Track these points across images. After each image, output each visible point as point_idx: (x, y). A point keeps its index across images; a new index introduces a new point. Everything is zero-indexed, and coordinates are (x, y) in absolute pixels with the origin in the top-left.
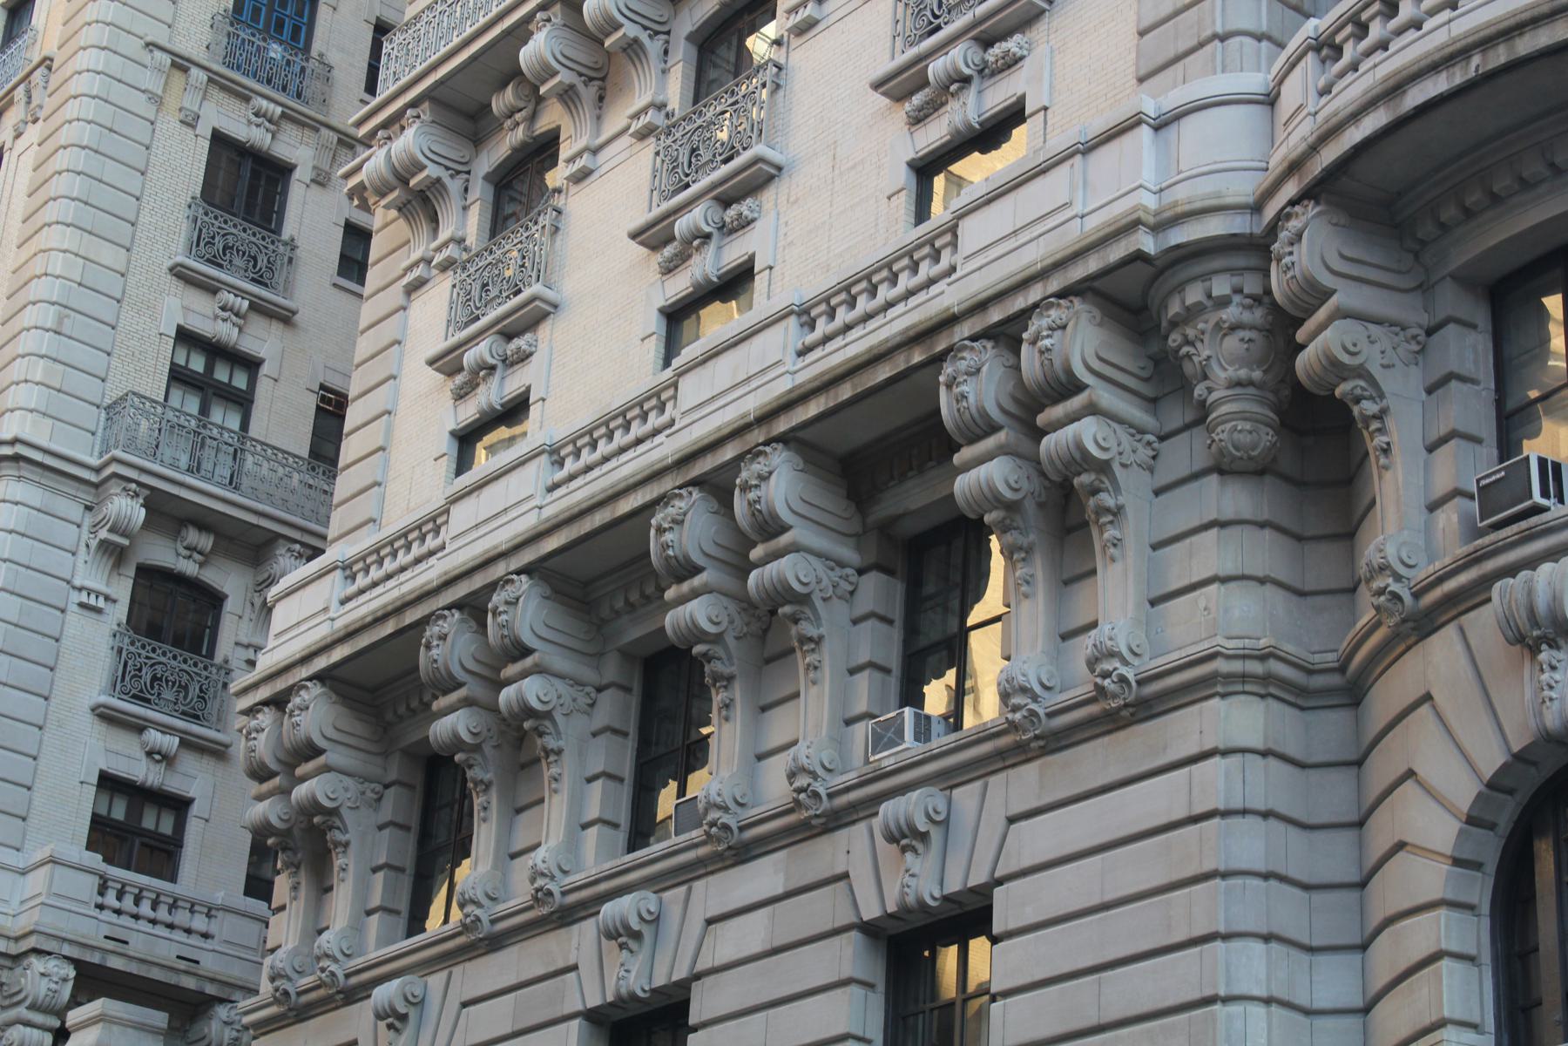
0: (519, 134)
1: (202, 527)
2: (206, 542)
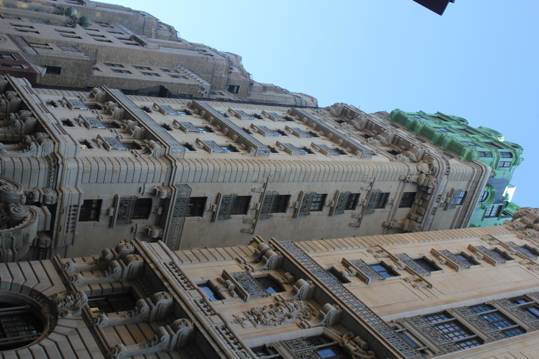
0: (282, 281)
1: (163, 211)
2: (160, 212)
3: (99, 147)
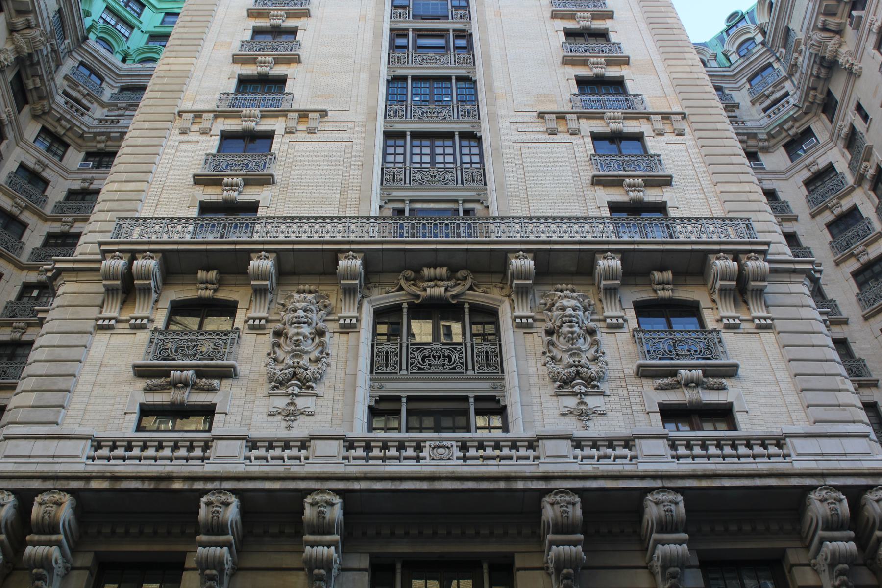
0: (208, 293)
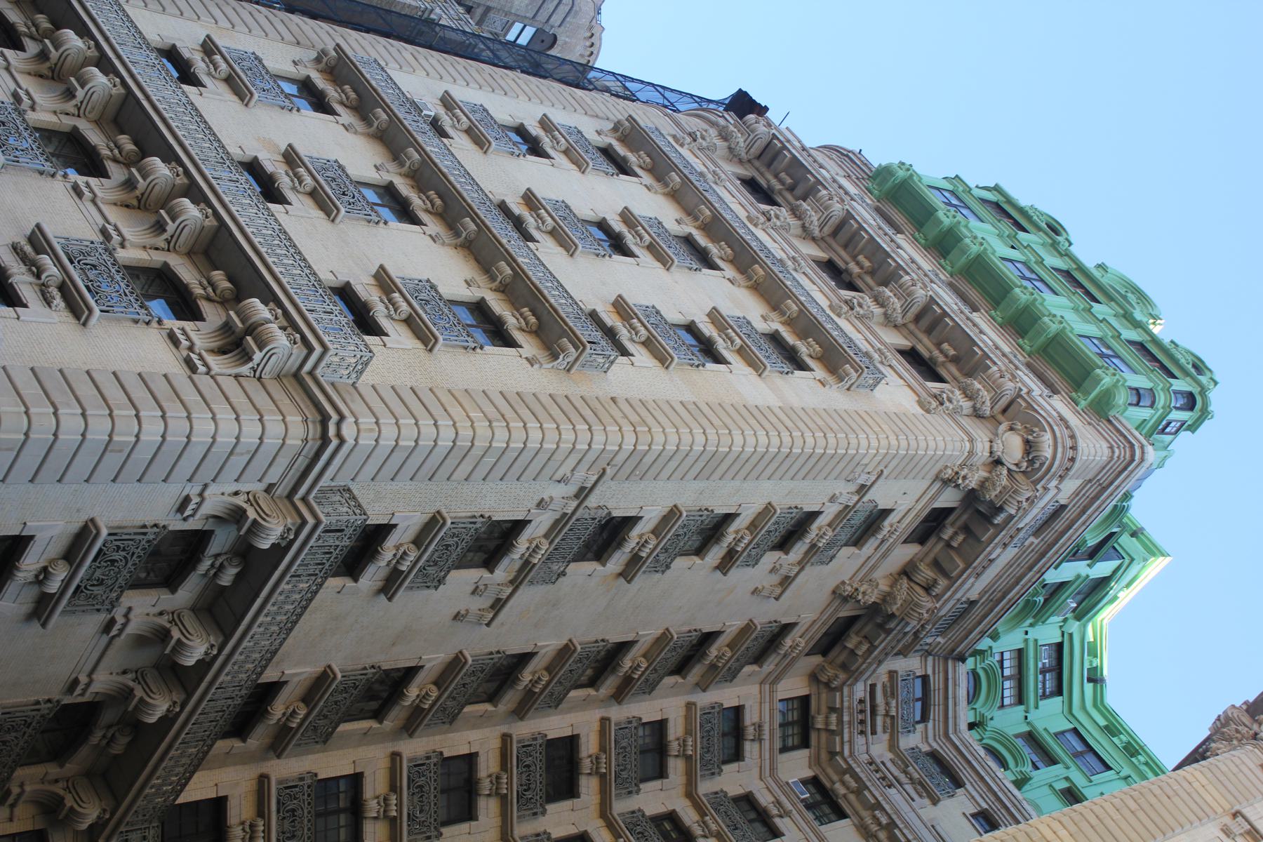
2: (226, 579)
3: (48, 302)
